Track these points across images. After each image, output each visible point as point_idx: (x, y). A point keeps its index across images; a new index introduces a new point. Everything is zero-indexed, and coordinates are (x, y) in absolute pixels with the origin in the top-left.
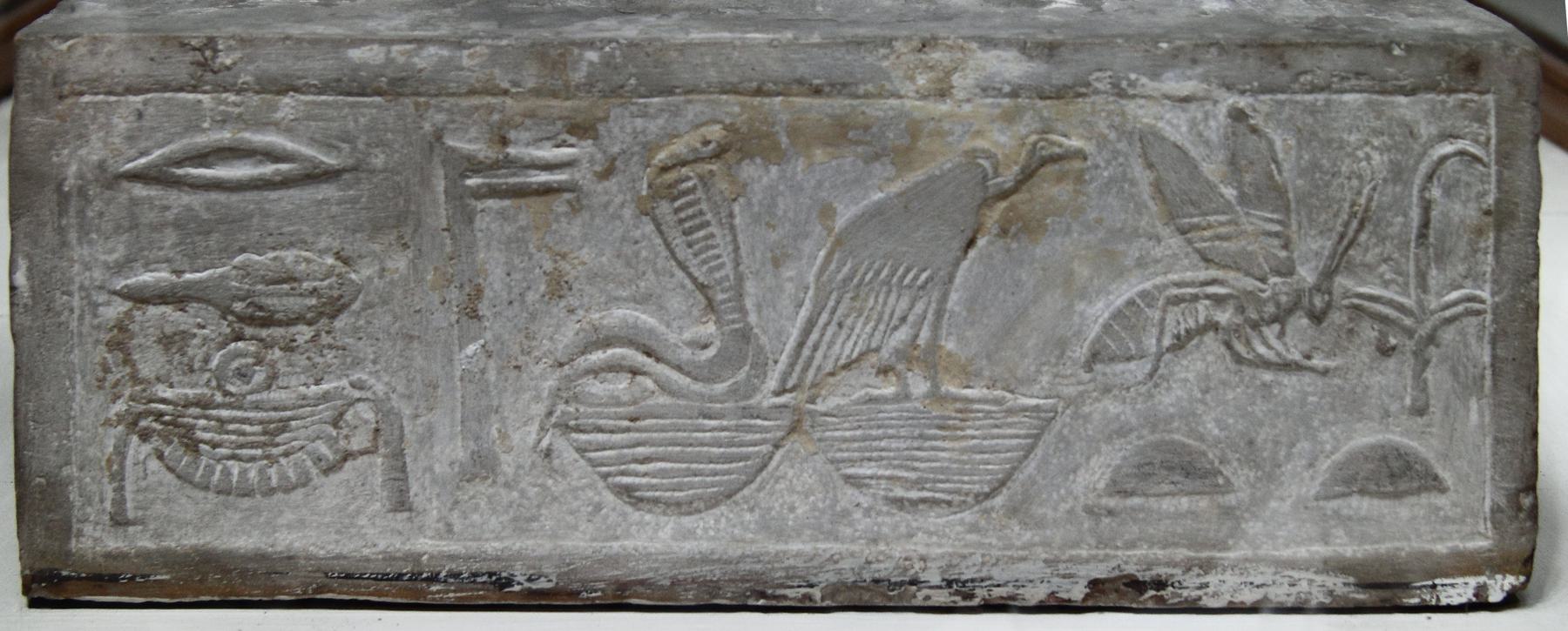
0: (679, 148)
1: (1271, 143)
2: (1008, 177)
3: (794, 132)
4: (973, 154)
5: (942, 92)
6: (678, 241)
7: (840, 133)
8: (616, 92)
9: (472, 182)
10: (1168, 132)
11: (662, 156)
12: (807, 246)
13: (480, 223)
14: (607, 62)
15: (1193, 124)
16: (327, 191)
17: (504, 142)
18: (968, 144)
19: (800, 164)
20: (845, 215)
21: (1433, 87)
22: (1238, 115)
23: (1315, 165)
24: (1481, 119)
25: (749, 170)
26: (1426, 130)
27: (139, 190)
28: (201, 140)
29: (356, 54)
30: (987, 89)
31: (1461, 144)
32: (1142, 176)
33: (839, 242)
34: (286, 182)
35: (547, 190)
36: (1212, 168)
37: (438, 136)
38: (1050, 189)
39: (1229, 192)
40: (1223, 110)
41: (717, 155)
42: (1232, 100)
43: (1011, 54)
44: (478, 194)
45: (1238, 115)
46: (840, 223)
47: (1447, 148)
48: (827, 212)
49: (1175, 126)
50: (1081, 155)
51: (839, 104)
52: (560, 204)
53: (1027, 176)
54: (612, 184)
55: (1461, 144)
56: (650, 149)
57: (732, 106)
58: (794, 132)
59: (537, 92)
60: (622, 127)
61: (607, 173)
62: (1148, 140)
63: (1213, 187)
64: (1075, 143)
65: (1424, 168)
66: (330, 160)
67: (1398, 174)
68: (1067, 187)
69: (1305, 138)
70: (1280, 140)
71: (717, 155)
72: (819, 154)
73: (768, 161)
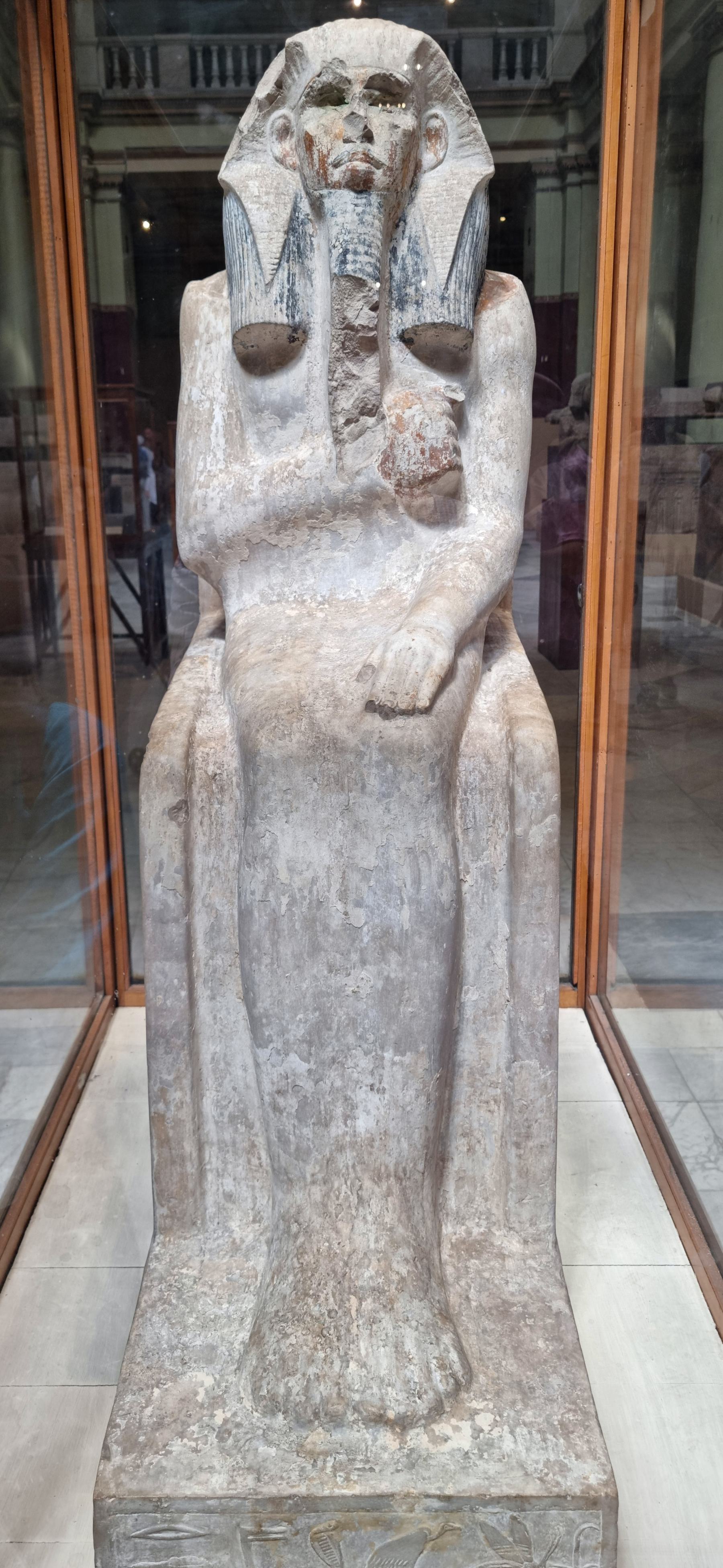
0: (321, 1527)
1: (525, 1526)
2: (434, 1536)
3: (360, 1523)
4: (422, 1529)
5: (411, 1510)
6: (321, 1553)
7: (376, 1522)
8: (299, 1512)
9: (250, 1537)
10: (490, 1523)
11: (315, 1529)
12: (365, 1554)
13: (253, 1548)
14: (296, 1504)
15: (498, 1520)
16: (201, 1540)
17: (261, 1526)
18: (421, 1526)
19: (363, 1532)
20: (378, 1545)
21: (582, 1509)
22: (514, 1518)
23: (540, 1531)
24: (598, 1518)
25: (345, 1533)
26: (578, 1521)
27: (137, 1540)
28: (158, 1527)
29: (210, 1502)
30: (427, 1509)
31: (590, 1525)
32: (481, 1536)
33: (376, 1553)
34: (187, 1538)
35: (275, 1539)
36: (505, 1533)
37: (238, 1525)
38: (448, 1538)
39: (511, 1539)
40: (508, 1516)
41: (334, 1529)
42: (510, 1513)
43: (435, 1500)
44: (252, 1540)
45: (514, 1518)
46: (376, 1548)
47: (585, 1526)
48: (372, 1545)
49: (492, 1521)
50: (459, 1529)
51: (376, 1514)
52: (280, 1543)
53: (440, 1535)
54: (298, 1537)
55: (590, 1525)
56: (310, 1528)
57: (339, 1516)
58: (360, 1523)
59: (272, 1512)
60: (302, 1522)
61: (297, 1533)
62: (483, 1526)
63: (505, 1538)
64: (457, 1525)
65: (577, 1532)
66: (201, 1532)
67: (569, 1533)
68: (455, 1537)
69: (536, 1524)
70: (529, 1525)
71: (334, 1529)
72: (369, 1528)
73: (351, 1530)
